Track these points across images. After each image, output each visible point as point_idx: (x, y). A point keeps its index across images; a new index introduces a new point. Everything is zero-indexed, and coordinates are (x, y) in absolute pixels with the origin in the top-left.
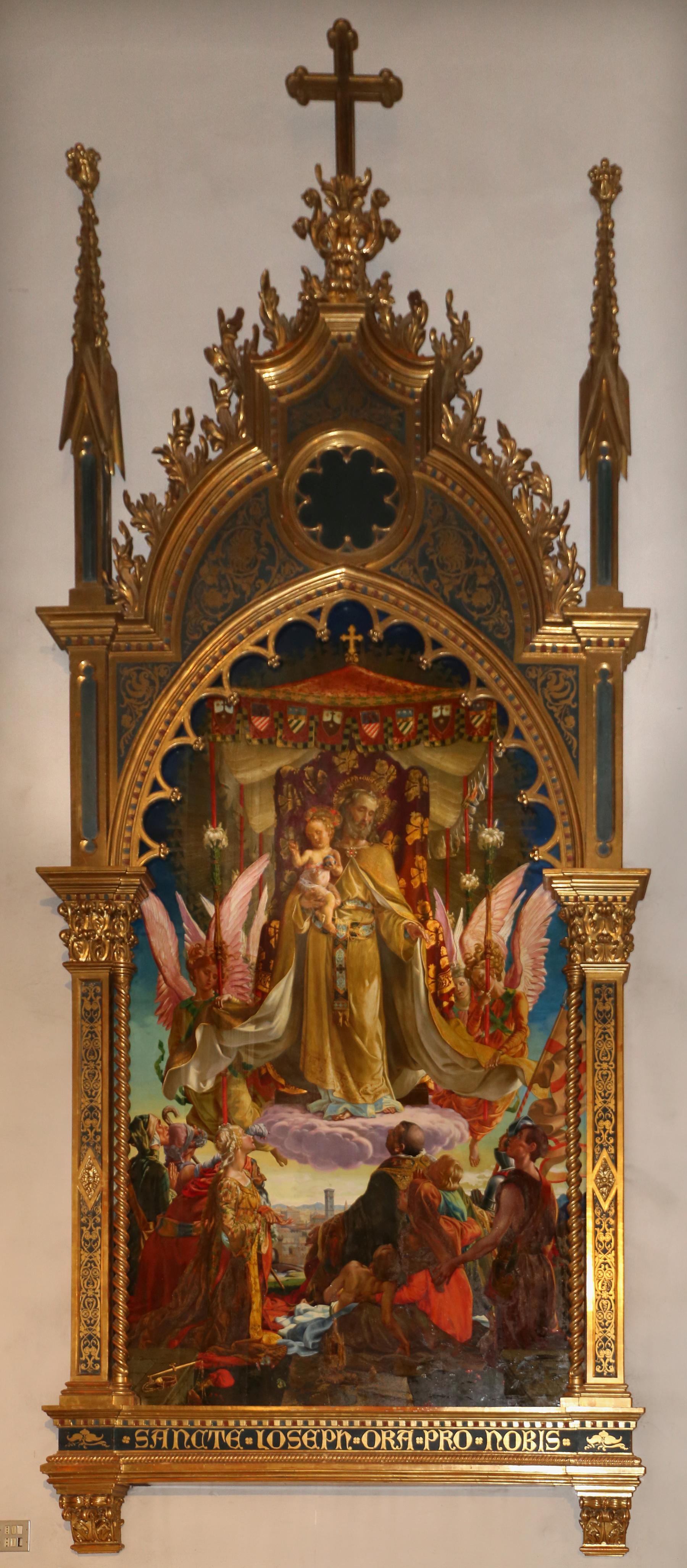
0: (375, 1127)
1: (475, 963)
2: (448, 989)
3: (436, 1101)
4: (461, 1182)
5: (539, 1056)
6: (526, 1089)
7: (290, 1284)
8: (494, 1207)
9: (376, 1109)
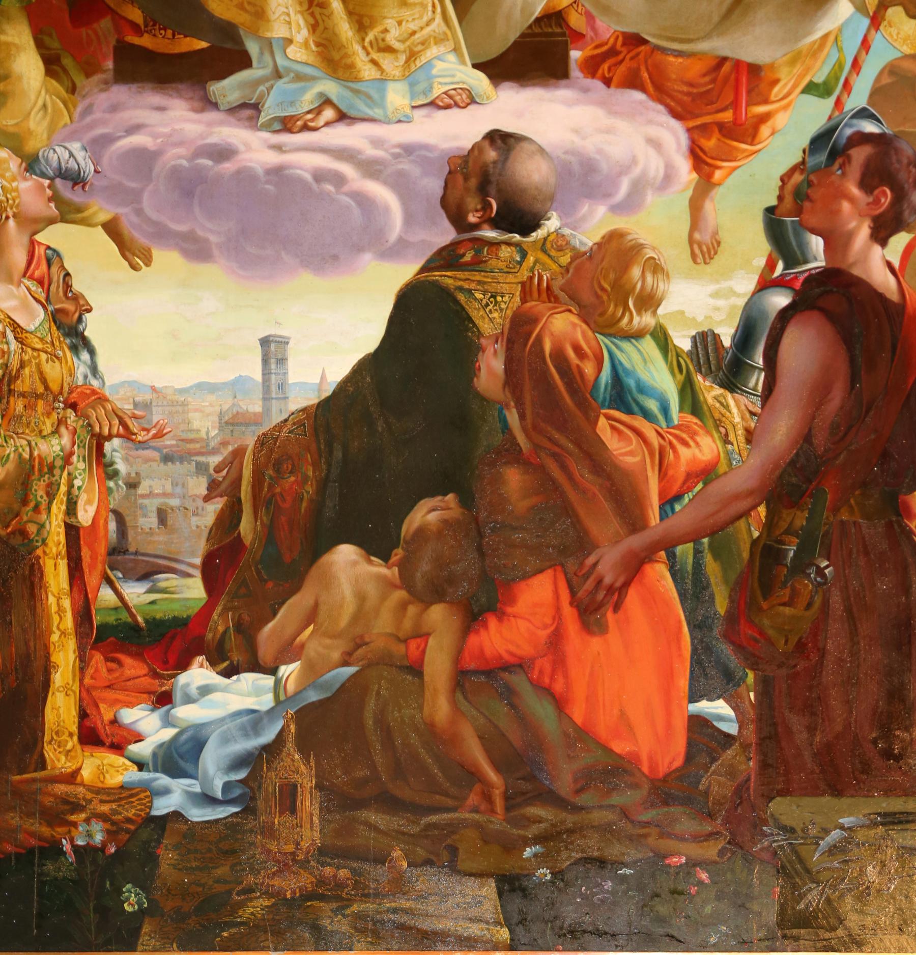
0: (408, 150)
3: (591, 67)
4: (660, 311)
6: (866, 22)
7: (159, 613)
8: (757, 380)
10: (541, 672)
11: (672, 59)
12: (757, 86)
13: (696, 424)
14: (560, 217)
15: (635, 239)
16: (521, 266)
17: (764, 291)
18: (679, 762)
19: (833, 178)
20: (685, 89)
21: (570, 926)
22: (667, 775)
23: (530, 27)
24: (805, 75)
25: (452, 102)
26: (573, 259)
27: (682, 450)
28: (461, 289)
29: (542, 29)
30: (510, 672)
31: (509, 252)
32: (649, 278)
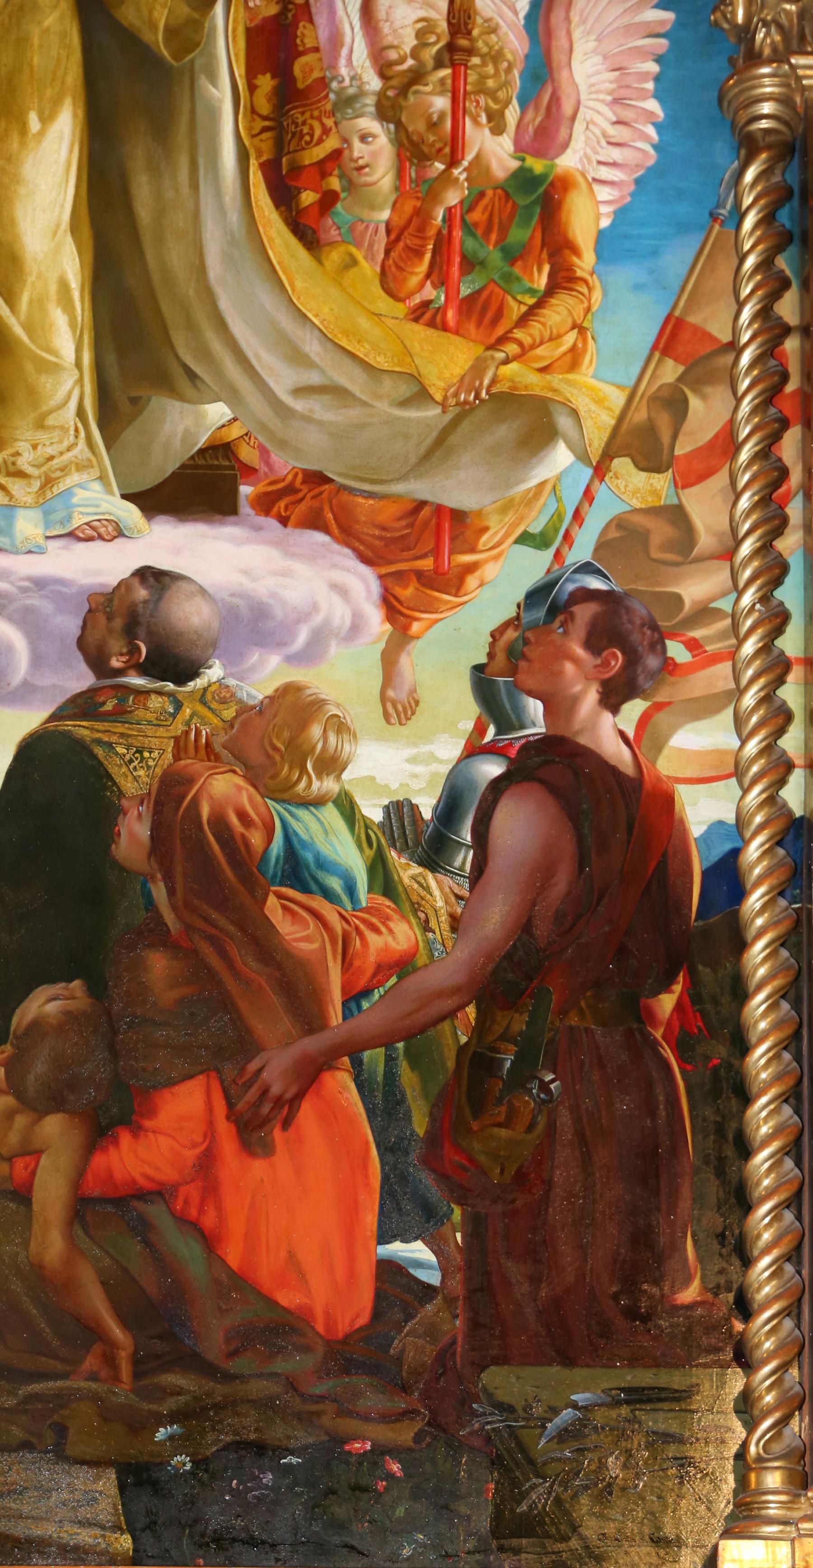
0: (40, 584)
1: (417, 76)
2: (318, 153)
4: (345, 776)
5: (636, 370)
6: (589, 472)
8: (464, 859)
9: (47, 525)
10: (186, 1202)
11: (361, 500)
12: (462, 533)
13: (389, 907)
14: (224, 665)
15: (314, 694)
16: (175, 718)
17: (472, 759)
18: (364, 1320)
19: (554, 636)
20: (377, 532)
21: (215, 1531)
22: (348, 1336)
23: (192, 458)
24: (518, 525)
25: (95, 534)
26: (239, 714)
27: (371, 937)
28: (99, 742)
29: (206, 461)
30: (146, 1201)
31: (160, 703)
32: (332, 739)
